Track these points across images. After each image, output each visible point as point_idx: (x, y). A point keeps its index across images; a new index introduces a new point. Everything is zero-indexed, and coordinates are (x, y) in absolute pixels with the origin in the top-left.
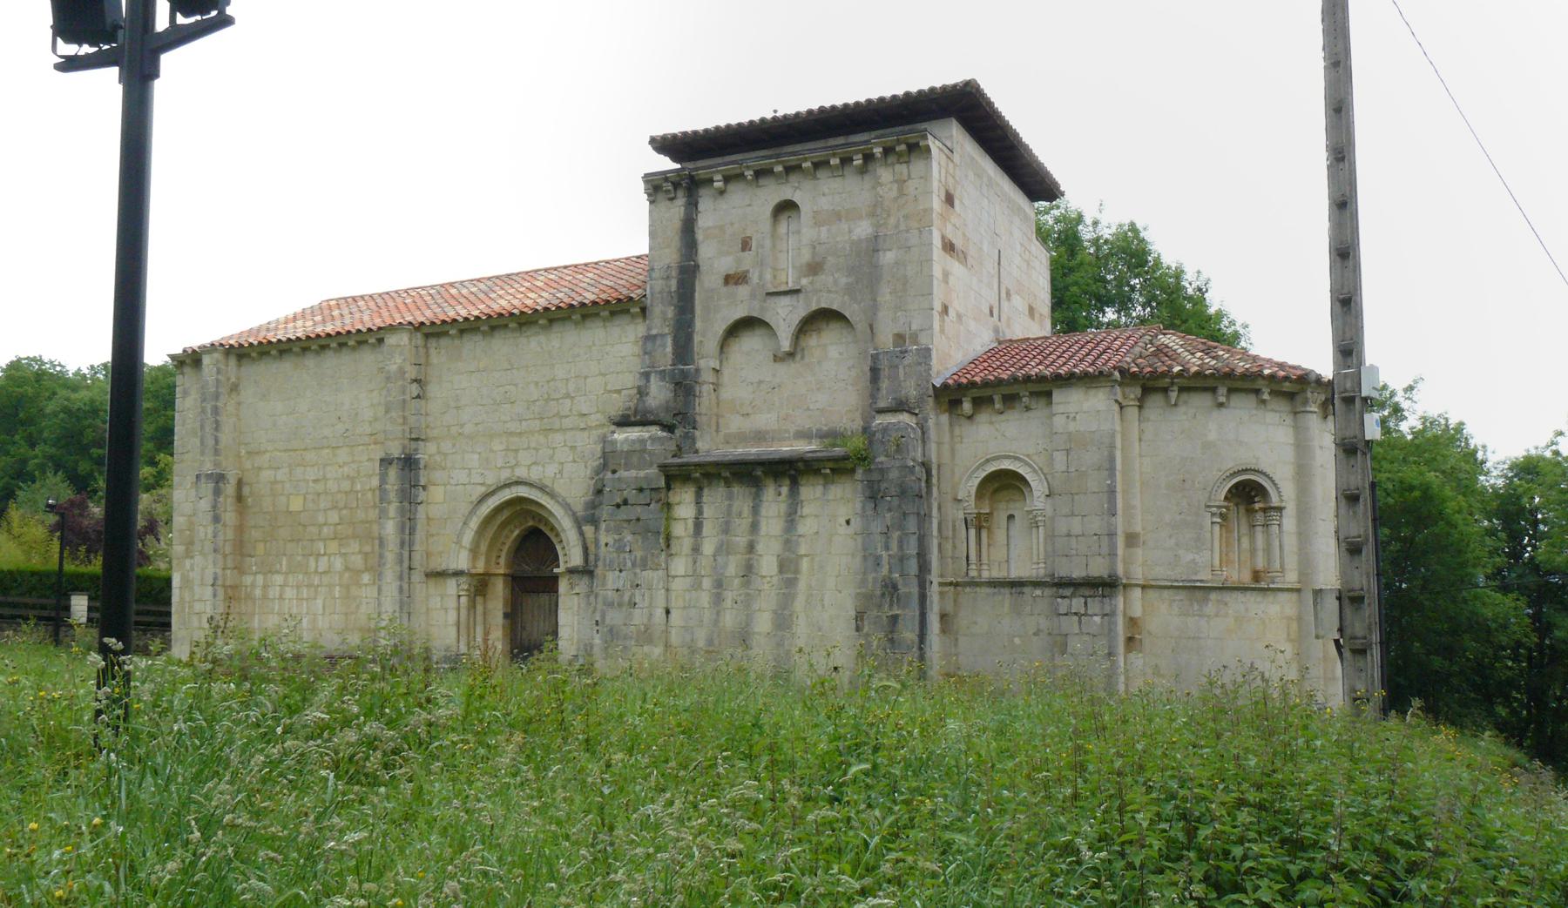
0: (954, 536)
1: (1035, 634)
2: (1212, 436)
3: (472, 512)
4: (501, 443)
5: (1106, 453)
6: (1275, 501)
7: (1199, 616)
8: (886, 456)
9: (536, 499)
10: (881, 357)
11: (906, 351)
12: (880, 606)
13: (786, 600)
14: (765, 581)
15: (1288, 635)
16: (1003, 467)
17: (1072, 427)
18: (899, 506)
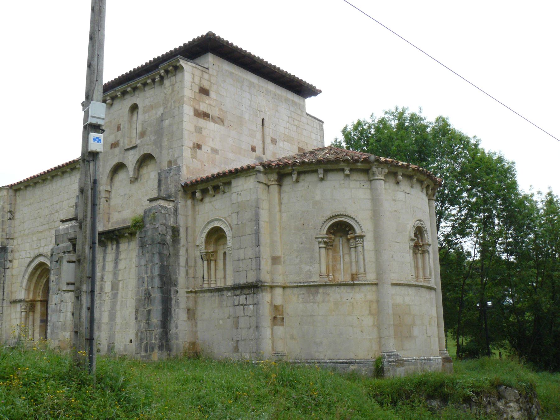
0: (195, 266)
1: (228, 318)
2: (318, 197)
3: (26, 271)
5: (254, 212)
6: (358, 232)
11: (171, 169)
13: (114, 304)
15: (370, 310)
16: (215, 225)
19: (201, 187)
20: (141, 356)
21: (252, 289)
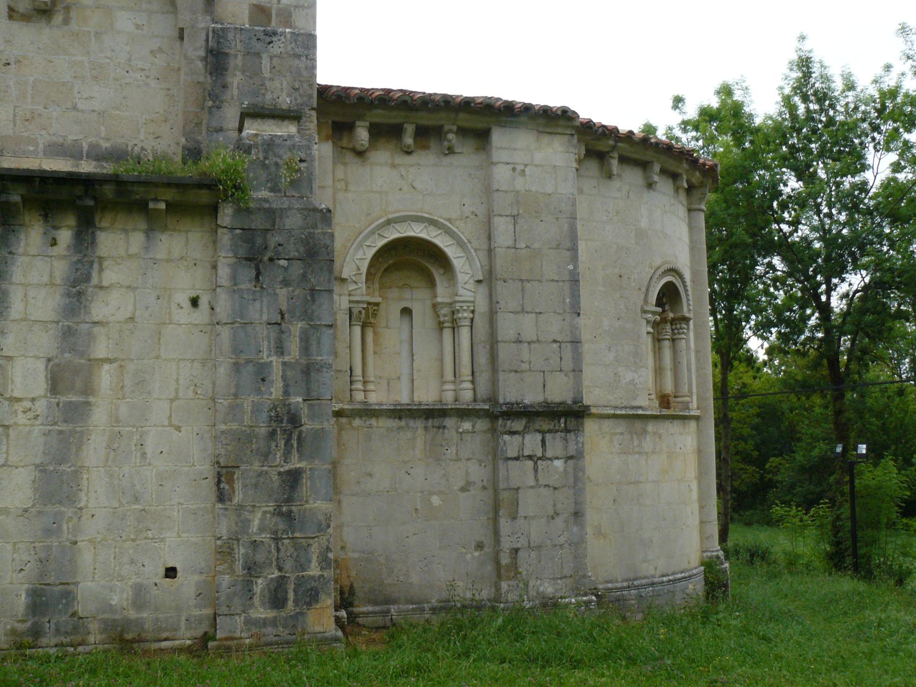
1: (463, 489)
2: (644, 223)
5: (566, 227)
7: (638, 453)
8: (272, 190)
10: (230, 36)
12: (266, 456)
14: (18, 407)
17: (520, 184)
18: (304, 276)
19: (380, 116)
20: (248, 622)
21: (562, 420)
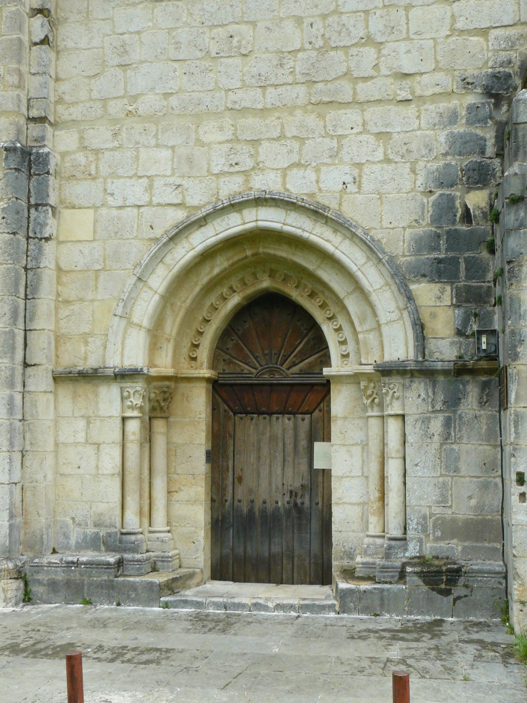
4: (221, 128)
9: (299, 232)
